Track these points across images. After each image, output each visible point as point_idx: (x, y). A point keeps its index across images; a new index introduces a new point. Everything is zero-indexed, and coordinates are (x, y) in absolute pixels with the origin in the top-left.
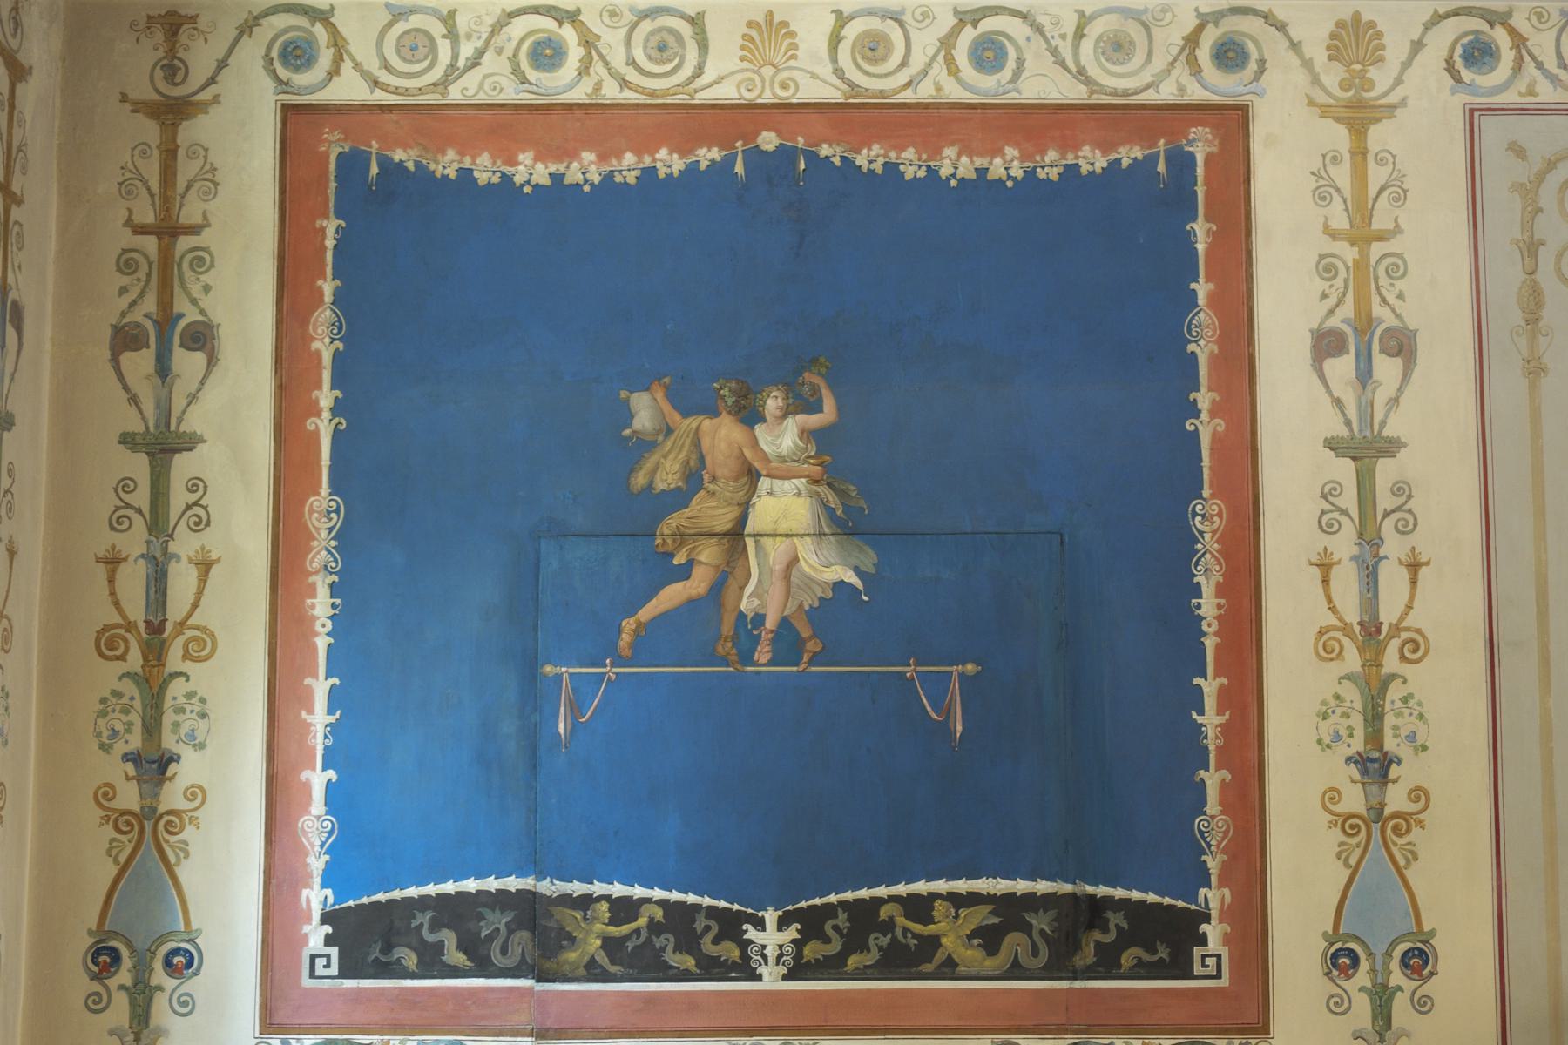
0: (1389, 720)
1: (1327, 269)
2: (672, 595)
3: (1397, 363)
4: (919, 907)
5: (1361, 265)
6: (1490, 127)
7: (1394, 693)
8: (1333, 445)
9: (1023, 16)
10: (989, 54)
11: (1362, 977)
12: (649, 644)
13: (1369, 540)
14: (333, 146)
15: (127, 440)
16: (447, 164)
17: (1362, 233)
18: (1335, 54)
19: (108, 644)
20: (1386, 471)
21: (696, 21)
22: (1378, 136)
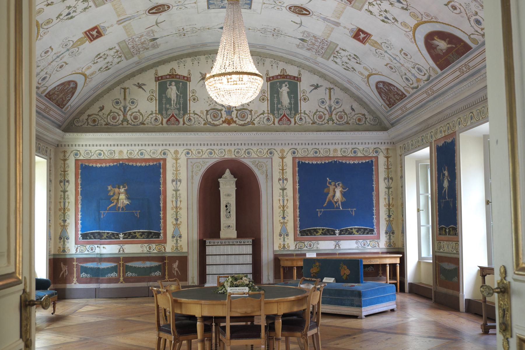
0: (178, 215)
1: (173, 174)
2: (112, 205)
3: (179, 183)
4: (135, 233)
5: (176, 173)
6: (189, 160)
7: (178, 213)
8: (173, 190)
9: (145, 150)
10: (142, 154)
11: (175, 238)
12: (111, 209)
13: (177, 199)
14: (80, 163)
15: (61, 191)
16: (91, 165)
17: (177, 170)
18: (174, 153)
19: (60, 210)
20: (178, 193)
21: (114, 151)
22: (178, 161)
